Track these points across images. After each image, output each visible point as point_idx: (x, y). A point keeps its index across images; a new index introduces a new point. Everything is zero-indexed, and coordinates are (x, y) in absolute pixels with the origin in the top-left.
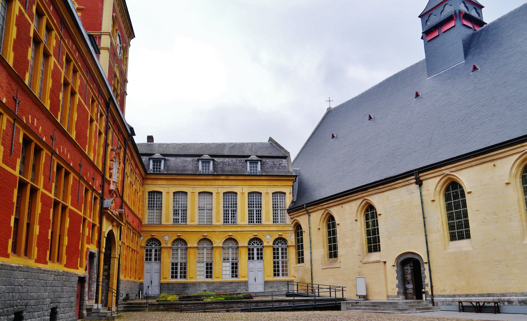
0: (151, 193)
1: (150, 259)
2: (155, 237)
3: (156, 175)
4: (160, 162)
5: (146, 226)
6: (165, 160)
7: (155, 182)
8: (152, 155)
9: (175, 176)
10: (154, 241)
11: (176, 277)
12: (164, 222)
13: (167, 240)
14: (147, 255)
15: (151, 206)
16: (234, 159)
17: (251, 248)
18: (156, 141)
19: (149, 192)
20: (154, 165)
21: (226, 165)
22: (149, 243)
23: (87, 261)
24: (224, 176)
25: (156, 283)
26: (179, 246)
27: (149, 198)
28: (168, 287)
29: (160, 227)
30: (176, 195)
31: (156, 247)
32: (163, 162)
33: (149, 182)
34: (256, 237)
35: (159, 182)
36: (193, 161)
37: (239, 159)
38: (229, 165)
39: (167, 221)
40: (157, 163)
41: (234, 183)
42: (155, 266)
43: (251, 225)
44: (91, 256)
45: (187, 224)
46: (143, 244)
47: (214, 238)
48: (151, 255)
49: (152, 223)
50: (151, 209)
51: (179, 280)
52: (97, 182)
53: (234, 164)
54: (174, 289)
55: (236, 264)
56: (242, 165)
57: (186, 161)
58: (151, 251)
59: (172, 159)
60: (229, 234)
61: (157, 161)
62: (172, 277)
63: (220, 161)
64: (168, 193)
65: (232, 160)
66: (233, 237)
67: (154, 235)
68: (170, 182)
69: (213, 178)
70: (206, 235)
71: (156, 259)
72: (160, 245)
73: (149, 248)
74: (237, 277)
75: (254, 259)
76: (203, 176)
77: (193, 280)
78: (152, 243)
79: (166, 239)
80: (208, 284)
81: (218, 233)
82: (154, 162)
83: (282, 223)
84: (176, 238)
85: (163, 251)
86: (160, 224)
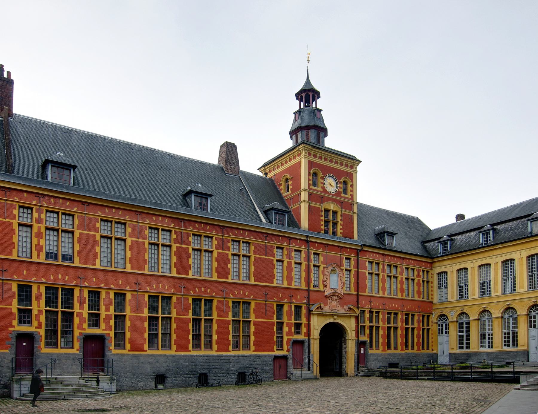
0: (439, 274)
1: (442, 333)
2: (444, 313)
3: (485, 248)
4: (447, 244)
5: (436, 304)
6: (451, 240)
7: (441, 263)
8: (440, 239)
9: (455, 255)
10: (443, 316)
11: (463, 348)
12: (450, 299)
13: (453, 316)
14: (439, 329)
15: (440, 286)
16: (517, 222)
17: (532, 315)
18: (467, 218)
19: (438, 274)
20: (443, 248)
21: (507, 231)
22: (441, 319)
23: (289, 347)
24: (500, 245)
25: (446, 354)
26: (464, 319)
27: (439, 279)
28: (455, 357)
29: (447, 304)
30: (481, 268)
31: (446, 321)
32: (449, 243)
33: (437, 264)
34: (535, 303)
35: (445, 263)
36: (476, 235)
37: (521, 221)
38: (511, 230)
39: (452, 297)
40: (445, 245)
41: (512, 249)
42: (442, 339)
43: (532, 290)
44: (300, 343)
45: (491, 296)
46: (435, 320)
47: (493, 309)
48: (442, 329)
49: (441, 301)
50: (441, 289)
51: (465, 350)
52: (299, 296)
53: (516, 227)
54: (460, 358)
55: (517, 333)
56: (524, 227)
57: (471, 236)
58: (442, 325)
59: (458, 237)
60: (507, 304)
61: (444, 243)
62: (460, 348)
63: (502, 227)
64: (452, 271)
65: (515, 224)
66: (511, 306)
67: (442, 312)
68: (454, 261)
69: (489, 249)
70: (485, 307)
71: (446, 333)
72: (448, 320)
73: (440, 323)
74: (509, 346)
75: (535, 327)
76: (480, 249)
77: (476, 350)
78: (443, 319)
79: (452, 314)
80: (488, 353)
81: (496, 304)
82: (484, 234)
83: (534, 289)
84: (460, 312)
85: (450, 325)
86: (447, 302)
